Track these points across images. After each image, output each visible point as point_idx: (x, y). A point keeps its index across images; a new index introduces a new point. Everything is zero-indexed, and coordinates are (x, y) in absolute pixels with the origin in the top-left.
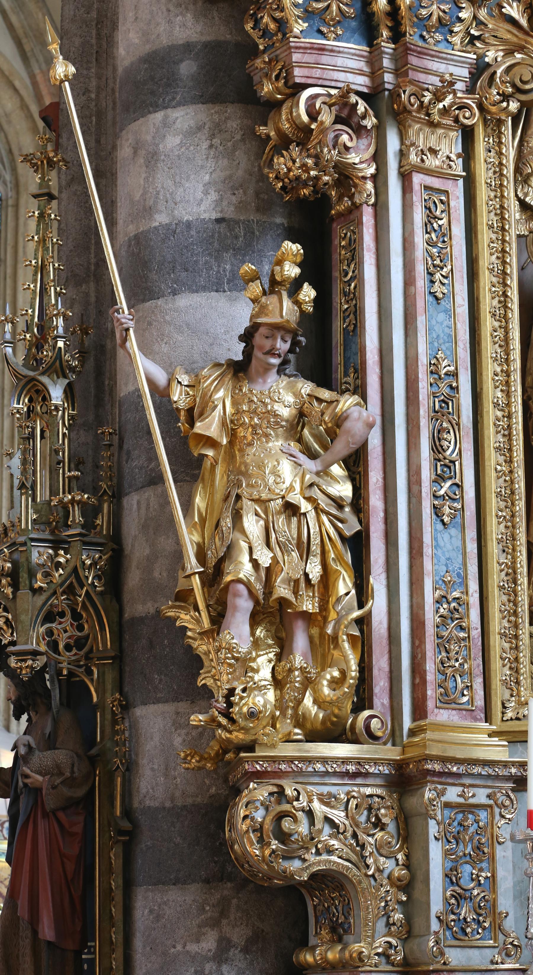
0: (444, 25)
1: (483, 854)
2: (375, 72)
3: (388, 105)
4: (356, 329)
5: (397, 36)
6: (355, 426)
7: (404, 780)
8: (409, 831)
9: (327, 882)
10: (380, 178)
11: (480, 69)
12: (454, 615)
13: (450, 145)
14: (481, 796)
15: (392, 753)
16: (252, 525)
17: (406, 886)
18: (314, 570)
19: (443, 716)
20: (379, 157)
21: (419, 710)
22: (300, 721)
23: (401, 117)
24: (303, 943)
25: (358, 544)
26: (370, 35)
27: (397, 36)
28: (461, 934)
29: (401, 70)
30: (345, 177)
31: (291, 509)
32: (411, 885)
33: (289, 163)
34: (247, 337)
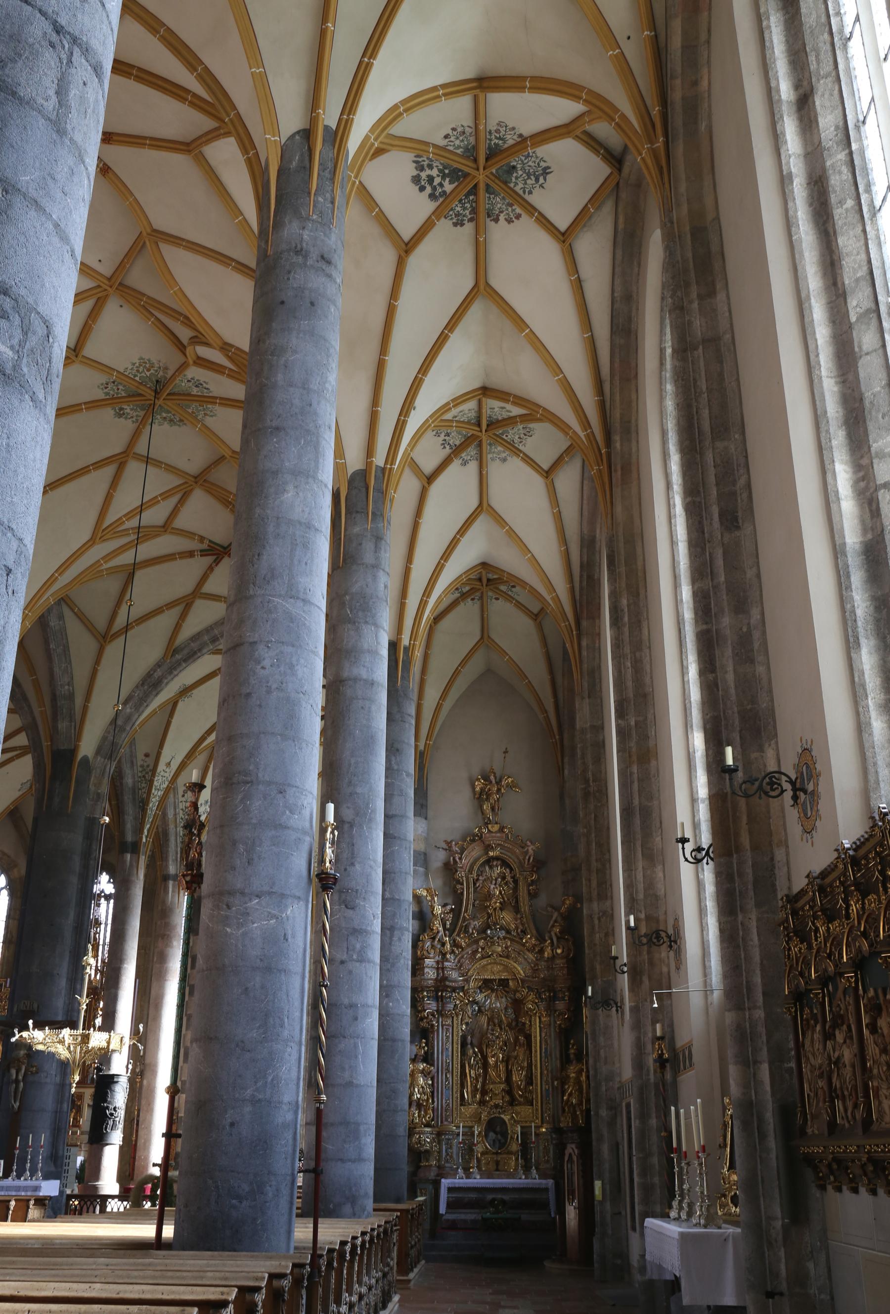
0: (450, 997)
1: (451, 1148)
2: (438, 1007)
3: (440, 1012)
4: (433, 1053)
5: (442, 1001)
6: (433, 1073)
7: (439, 1134)
8: (439, 1143)
9: (427, 1151)
10: (438, 1026)
11: (456, 1005)
12: (448, 1105)
13: (449, 1022)
14: (451, 1137)
15: (437, 1129)
16: (416, 1090)
17: (439, 1152)
18: (426, 1097)
19: (446, 1123)
20: (438, 1022)
21: (442, 1122)
22: (422, 1123)
23: (442, 1016)
24: (420, 1161)
25: (433, 1092)
26: (438, 1001)
27: (442, 1001)
28: (447, 1161)
29: (443, 1007)
30: (433, 1025)
31: (423, 1087)
32: (440, 1152)
33: (424, 1024)
34: (416, 1056)
